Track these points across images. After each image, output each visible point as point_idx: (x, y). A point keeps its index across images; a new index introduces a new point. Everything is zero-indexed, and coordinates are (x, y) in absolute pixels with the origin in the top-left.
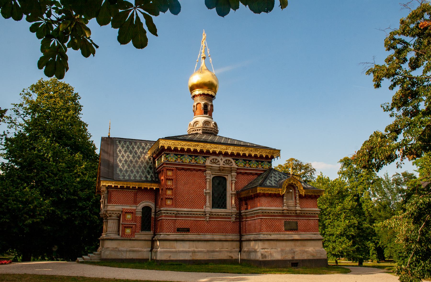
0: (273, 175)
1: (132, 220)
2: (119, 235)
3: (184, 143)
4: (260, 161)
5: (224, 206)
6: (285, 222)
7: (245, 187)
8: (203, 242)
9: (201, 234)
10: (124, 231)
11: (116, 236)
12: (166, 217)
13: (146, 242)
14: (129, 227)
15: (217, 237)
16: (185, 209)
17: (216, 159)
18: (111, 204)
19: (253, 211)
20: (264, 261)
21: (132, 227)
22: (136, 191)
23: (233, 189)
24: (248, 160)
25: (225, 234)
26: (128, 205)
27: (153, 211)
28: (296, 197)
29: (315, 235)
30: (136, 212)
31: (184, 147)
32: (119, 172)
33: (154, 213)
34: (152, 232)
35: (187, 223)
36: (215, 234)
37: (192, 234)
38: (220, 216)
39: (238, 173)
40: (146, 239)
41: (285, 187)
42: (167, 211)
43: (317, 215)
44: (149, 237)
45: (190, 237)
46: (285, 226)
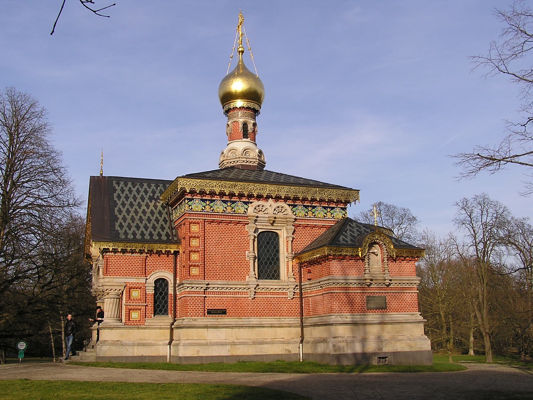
0: (348, 227)
2: (121, 320)
3: (214, 183)
5: (275, 275)
7: (307, 246)
10: (129, 315)
16: (219, 282)
18: (108, 277)
23: (290, 250)
32: (119, 229)
33: (172, 289)
41: (367, 246)
42: (192, 284)
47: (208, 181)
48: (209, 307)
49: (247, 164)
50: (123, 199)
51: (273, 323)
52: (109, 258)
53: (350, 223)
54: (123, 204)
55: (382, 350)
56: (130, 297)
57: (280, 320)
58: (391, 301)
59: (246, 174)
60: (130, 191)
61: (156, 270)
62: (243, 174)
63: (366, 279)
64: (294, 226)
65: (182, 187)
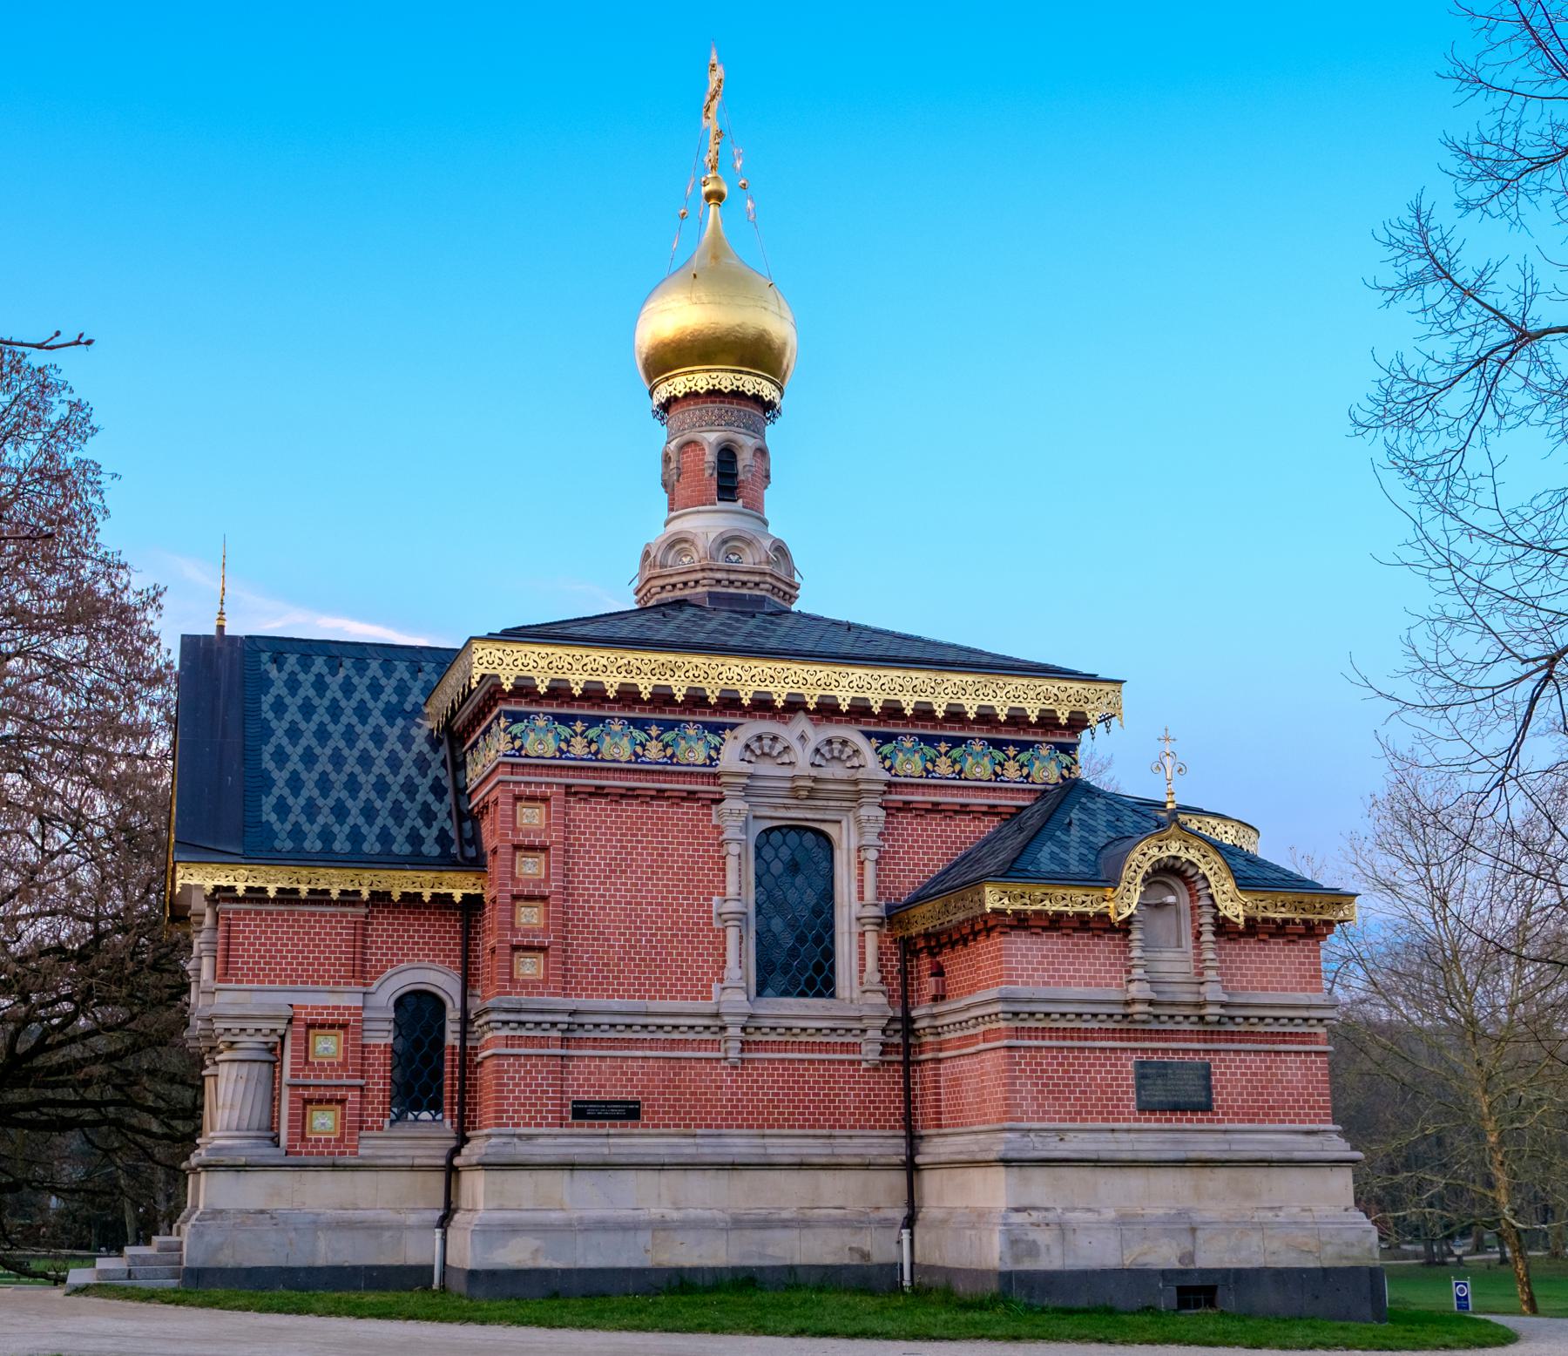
1: (343, 1065)
2: (275, 1140)
4: (1015, 743)
5: (820, 982)
6: (1141, 1065)
7: (933, 880)
8: (710, 1174)
9: (699, 1131)
10: (300, 1122)
11: (260, 1151)
12: (513, 1046)
13: (419, 1177)
14: (329, 1101)
15: (783, 1146)
16: (616, 1004)
17: (775, 739)
19: (969, 1008)
20: (1027, 1273)
21: (342, 1102)
22: (363, 911)
23: (870, 894)
24: (947, 739)
25: (825, 1132)
26: (320, 987)
27: (453, 1014)
28: (1200, 934)
29: (1312, 1139)
30: (363, 1021)
31: (603, 678)
32: (273, 817)
33: (457, 1027)
35: (625, 1073)
36: (775, 1131)
37: (651, 1131)
38: (803, 1038)
39: (891, 810)
40: (417, 1162)
41: (1139, 880)
42: (519, 1011)
43: (1321, 1030)
44: (435, 1152)
45: (642, 1150)
46: (1140, 1088)
47: (578, 652)
48: (578, 1092)
49: (732, 590)
50: (293, 714)
51: (805, 1151)
52: (234, 919)
53: (1083, 800)
54: (294, 733)
55: (1193, 1262)
56: (307, 1057)
57: (832, 1141)
58: (1227, 1081)
59: (721, 624)
60: (320, 686)
61: (402, 961)
62: (710, 626)
63: (1133, 1002)
64: (884, 808)
65: (486, 672)
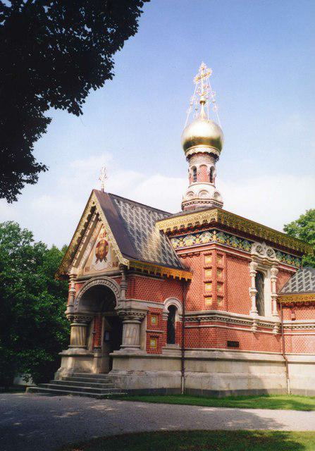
13: (175, 361)
21: (158, 337)
23: (274, 291)
34: (178, 346)
